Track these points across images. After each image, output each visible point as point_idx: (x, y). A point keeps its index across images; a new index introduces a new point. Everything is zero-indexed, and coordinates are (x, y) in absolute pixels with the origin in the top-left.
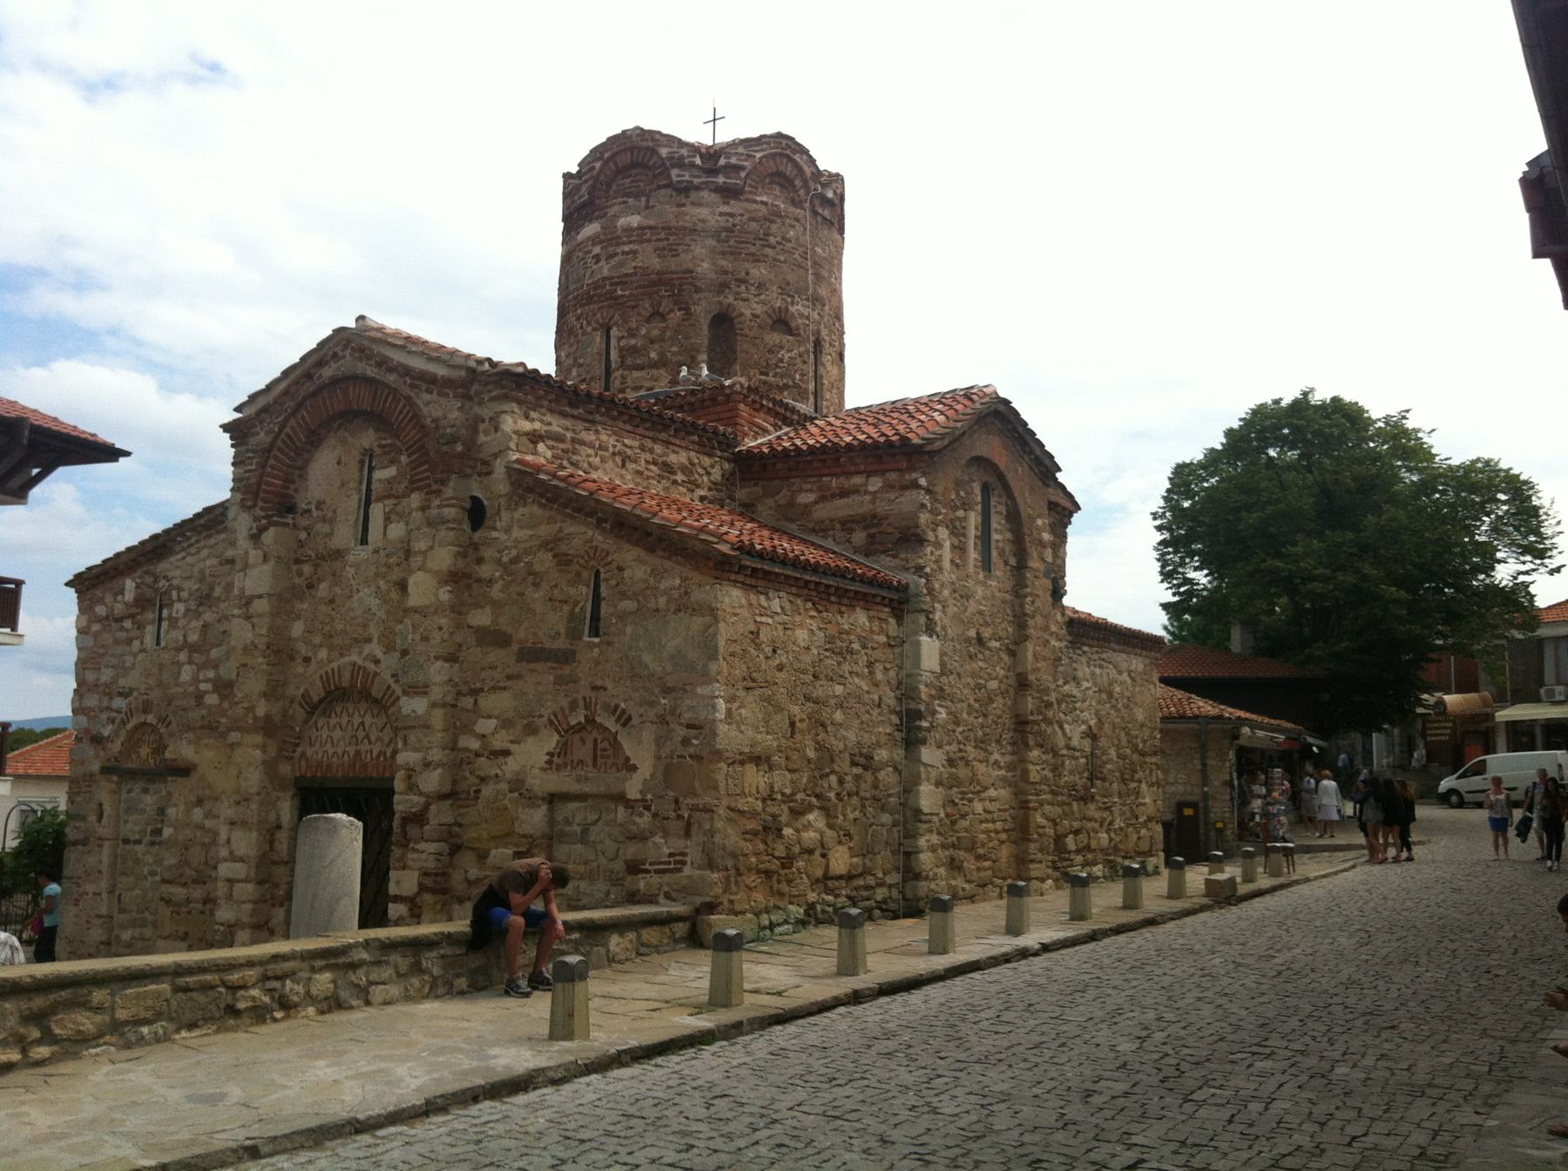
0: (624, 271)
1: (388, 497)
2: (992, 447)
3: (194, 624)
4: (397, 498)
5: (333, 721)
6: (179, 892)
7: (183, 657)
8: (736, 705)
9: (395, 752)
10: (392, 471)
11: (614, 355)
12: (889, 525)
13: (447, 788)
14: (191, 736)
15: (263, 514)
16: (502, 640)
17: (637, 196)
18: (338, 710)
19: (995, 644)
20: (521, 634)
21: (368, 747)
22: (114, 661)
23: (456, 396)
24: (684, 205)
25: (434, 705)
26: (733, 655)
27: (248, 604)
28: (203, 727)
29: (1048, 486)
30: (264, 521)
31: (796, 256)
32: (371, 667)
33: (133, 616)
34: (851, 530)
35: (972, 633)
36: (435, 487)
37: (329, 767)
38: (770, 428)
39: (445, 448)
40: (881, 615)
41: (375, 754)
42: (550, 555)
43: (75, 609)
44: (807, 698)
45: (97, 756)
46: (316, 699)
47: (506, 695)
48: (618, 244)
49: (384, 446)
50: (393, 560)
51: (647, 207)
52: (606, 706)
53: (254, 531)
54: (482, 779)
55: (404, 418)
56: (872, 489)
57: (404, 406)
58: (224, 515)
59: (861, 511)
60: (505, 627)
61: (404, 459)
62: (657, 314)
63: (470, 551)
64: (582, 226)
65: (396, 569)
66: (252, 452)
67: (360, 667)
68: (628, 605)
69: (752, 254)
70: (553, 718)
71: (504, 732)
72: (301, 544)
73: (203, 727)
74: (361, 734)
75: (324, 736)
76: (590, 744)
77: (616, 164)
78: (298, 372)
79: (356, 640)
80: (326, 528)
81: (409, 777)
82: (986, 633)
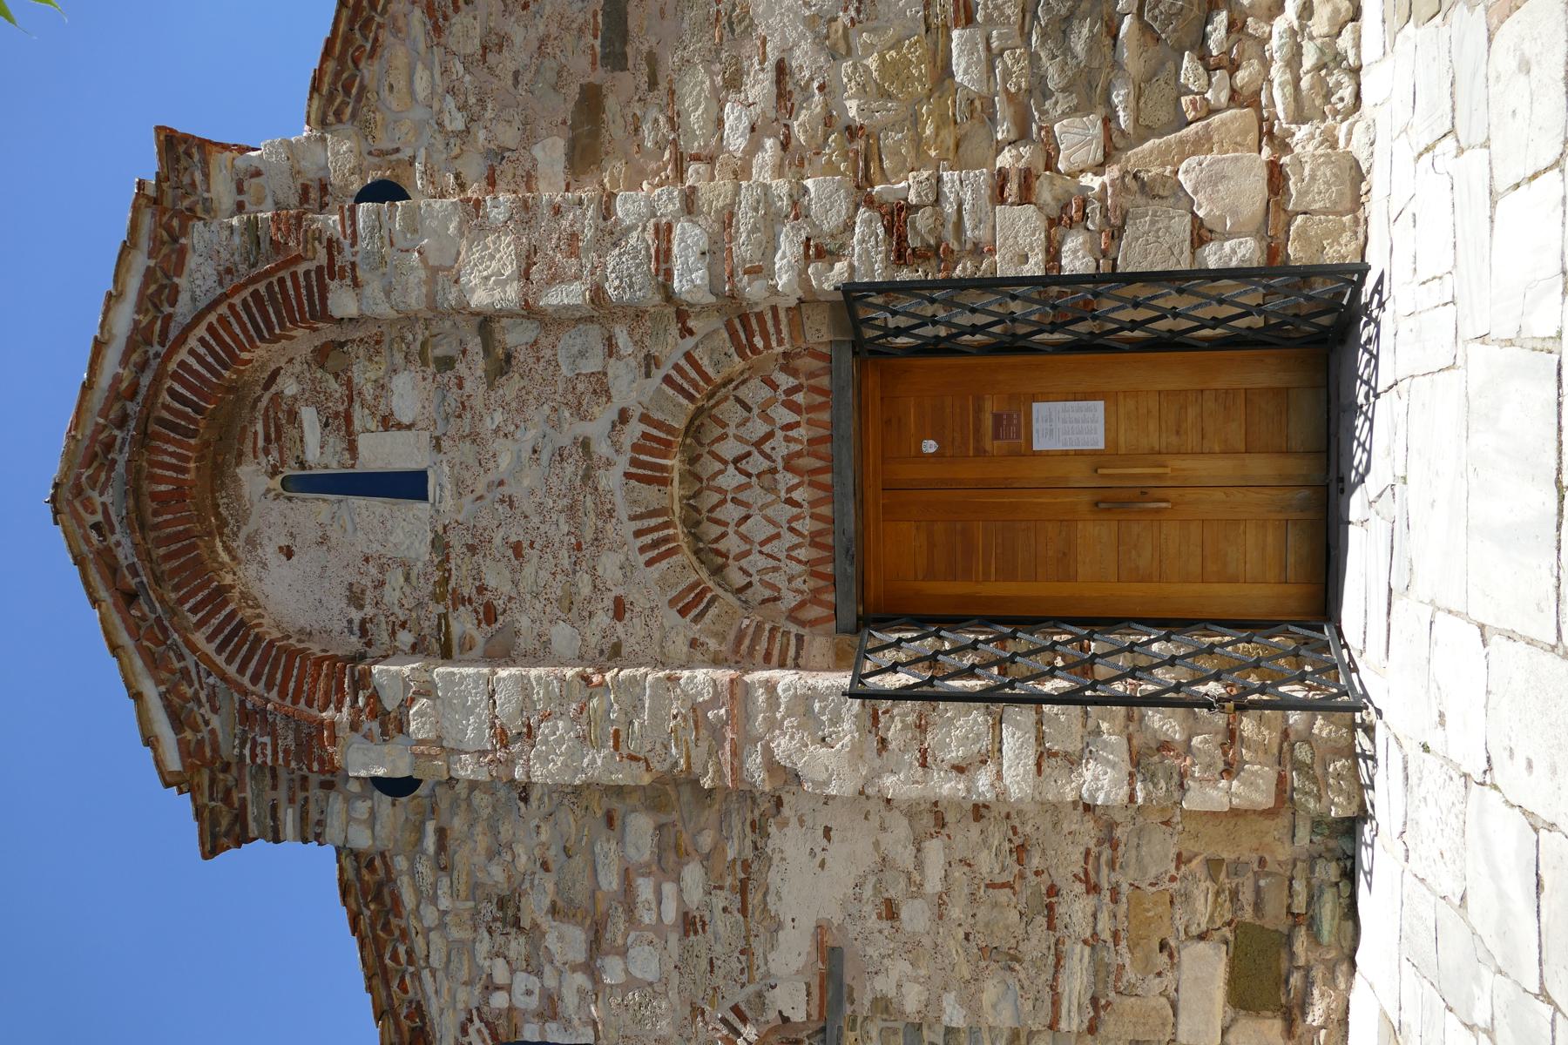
3: (551, 941)
4: (351, 400)
5: (732, 544)
6: (1076, 982)
10: (308, 416)
14: (758, 947)
18: (716, 530)
21: (779, 434)
23: (184, 230)
28: (743, 910)
32: (635, 429)
37: (814, 541)
41: (791, 417)
49: (267, 439)
57: (192, 352)
58: (356, 855)
60: (564, 106)
65: (468, 385)
66: (242, 745)
67: (634, 462)
73: (743, 910)
74: (757, 463)
78: (116, 619)
79: (587, 477)
80: (396, 578)
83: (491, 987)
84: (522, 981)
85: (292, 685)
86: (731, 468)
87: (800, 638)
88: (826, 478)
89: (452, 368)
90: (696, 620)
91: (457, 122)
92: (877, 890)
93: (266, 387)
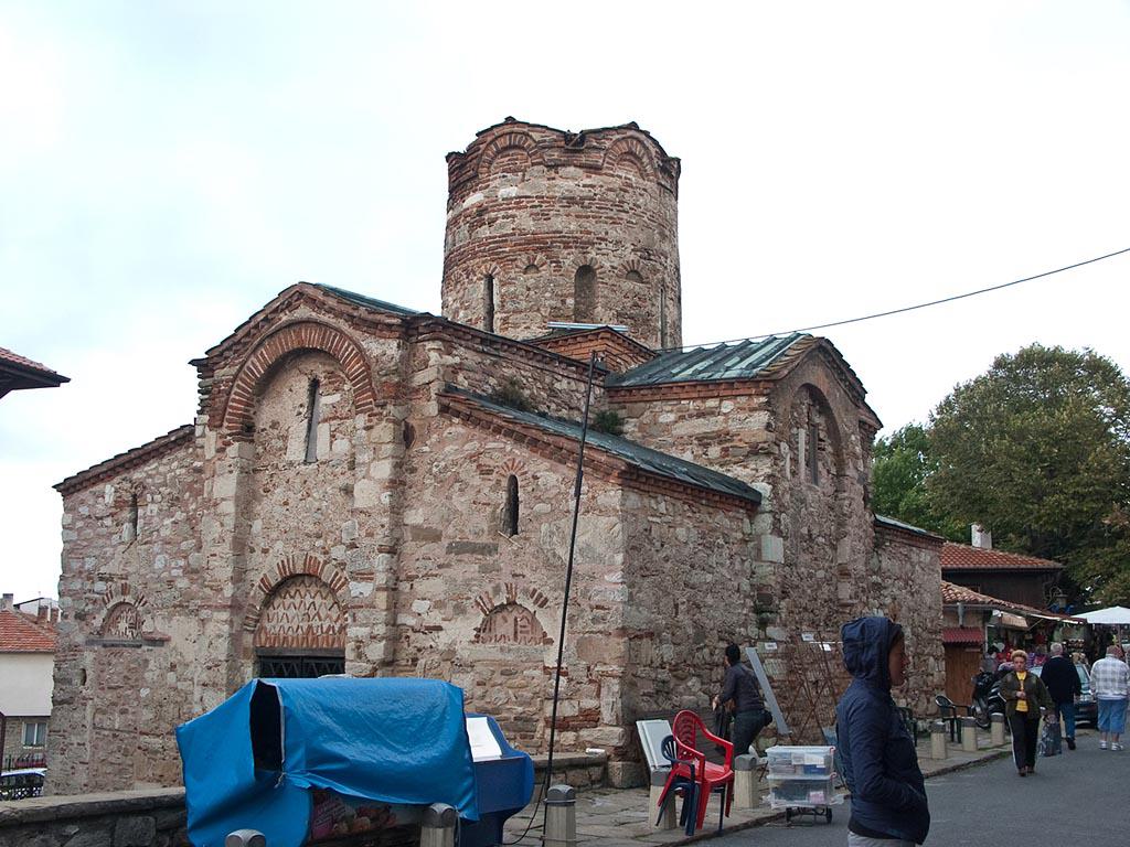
0: (505, 232)
1: (334, 418)
2: (818, 376)
5: (288, 601)
7: (156, 548)
8: (636, 589)
9: (343, 628)
10: (336, 397)
11: (496, 300)
12: (740, 440)
13: (390, 658)
15: (229, 432)
16: (435, 537)
17: (514, 172)
18: (292, 594)
19: (821, 540)
20: (451, 530)
22: (97, 553)
24: (554, 179)
25: (378, 589)
26: (633, 548)
27: (216, 505)
28: (175, 606)
29: (859, 407)
30: (229, 438)
31: (645, 219)
32: (321, 559)
33: (112, 515)
34: (706, 445)
35: (805, 531)
36: (376, 410)
38: (629, 360)
39: (384, 379)
40: (738, 515)
41: (324, 630)
42: (474, 465)
43: (61, 511)
44: (686, 585)
45: (81, 629)
46: (273, 583)
47: (438, 580)
48: (499, 210)
50: (339, 470)
51: (523, 181)
52: (525, 591)
53: (220, 445)
54: (419, 650)
55: (347, 357)
56: (724, 410)
58: (193, 432)
59: (716, 429)
61: (346, 387)
62: (531, 267)
63: (402, 466)
64: (468, 194)
68: (539, 507)
69: (611, 218)
70: (479, 600)
71: (436, 611)
72: (258, 457)
75: (280, 614)
76: (511, 620)
77: (496, 146)
79: (307, 535)
80: (280, 444)
81: (358, 648)
82: (815, 532)
83: (152, 494)
84: (155, 508)
85: (234, 404)
86: (311, 600)
87: (253, 632)
88: (305, 645)
89: (349, 469)
90: (260, 587)
91: (435, 470)
92: (179, 662)
93: (347, 375)
